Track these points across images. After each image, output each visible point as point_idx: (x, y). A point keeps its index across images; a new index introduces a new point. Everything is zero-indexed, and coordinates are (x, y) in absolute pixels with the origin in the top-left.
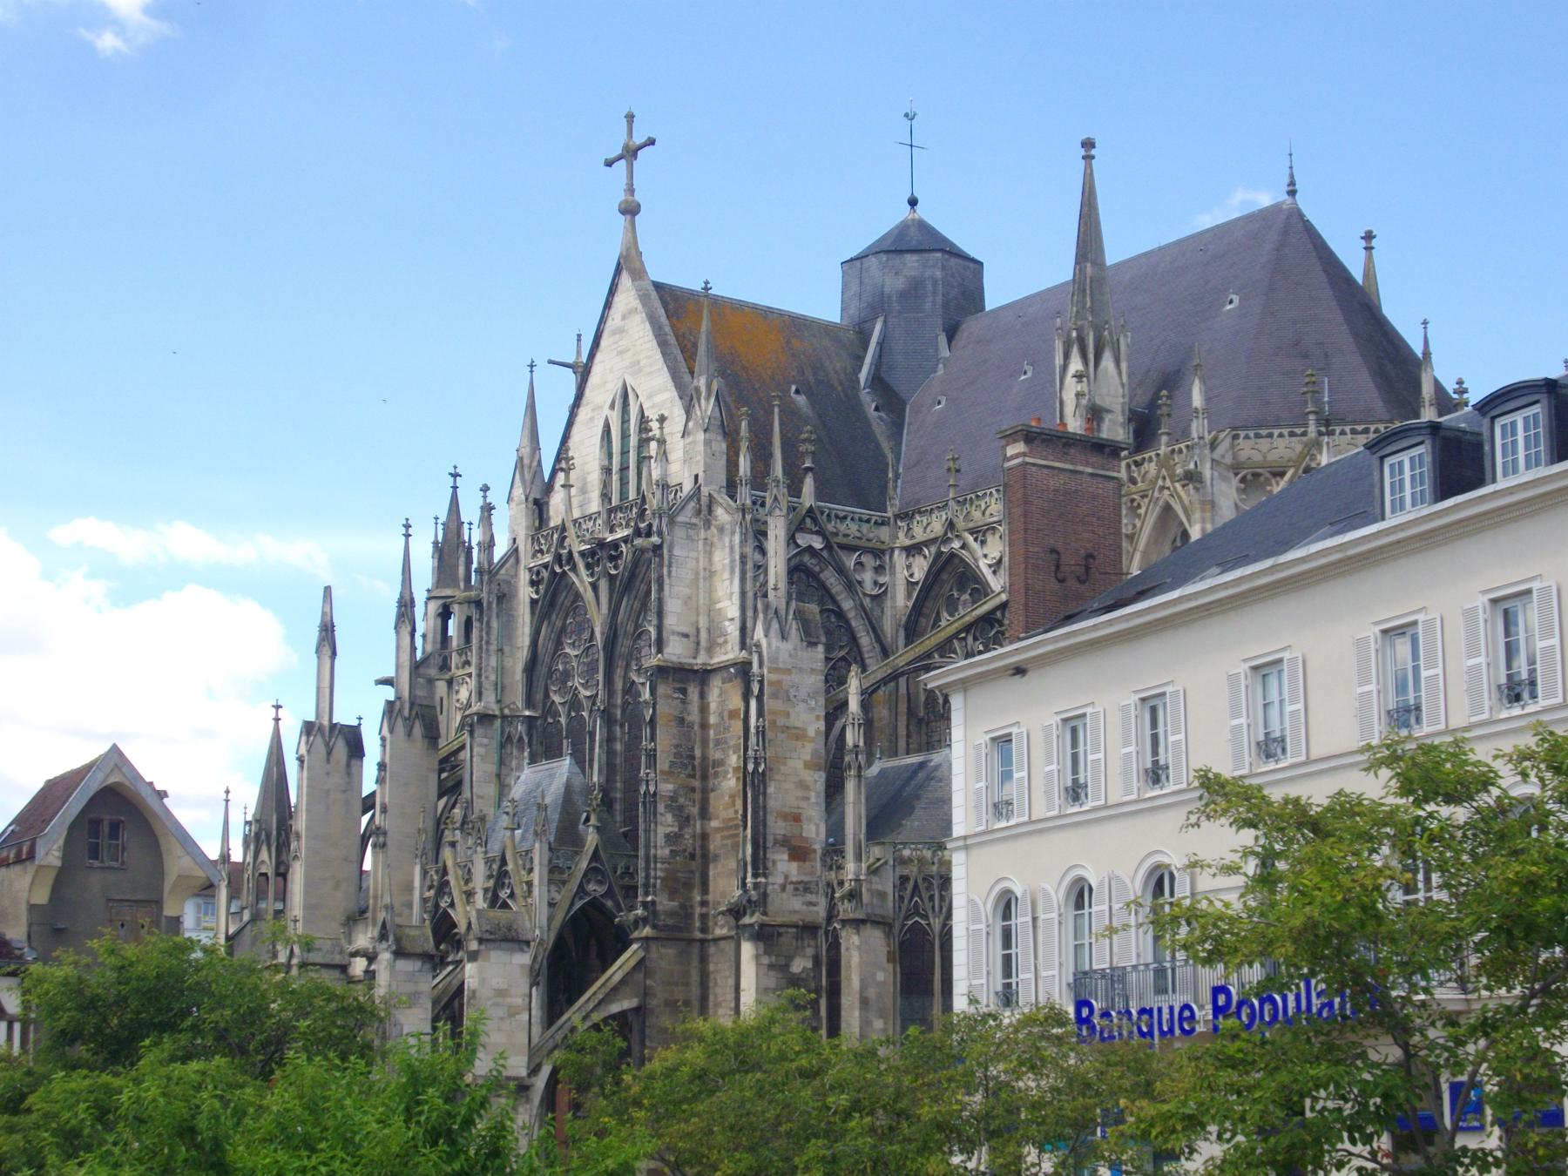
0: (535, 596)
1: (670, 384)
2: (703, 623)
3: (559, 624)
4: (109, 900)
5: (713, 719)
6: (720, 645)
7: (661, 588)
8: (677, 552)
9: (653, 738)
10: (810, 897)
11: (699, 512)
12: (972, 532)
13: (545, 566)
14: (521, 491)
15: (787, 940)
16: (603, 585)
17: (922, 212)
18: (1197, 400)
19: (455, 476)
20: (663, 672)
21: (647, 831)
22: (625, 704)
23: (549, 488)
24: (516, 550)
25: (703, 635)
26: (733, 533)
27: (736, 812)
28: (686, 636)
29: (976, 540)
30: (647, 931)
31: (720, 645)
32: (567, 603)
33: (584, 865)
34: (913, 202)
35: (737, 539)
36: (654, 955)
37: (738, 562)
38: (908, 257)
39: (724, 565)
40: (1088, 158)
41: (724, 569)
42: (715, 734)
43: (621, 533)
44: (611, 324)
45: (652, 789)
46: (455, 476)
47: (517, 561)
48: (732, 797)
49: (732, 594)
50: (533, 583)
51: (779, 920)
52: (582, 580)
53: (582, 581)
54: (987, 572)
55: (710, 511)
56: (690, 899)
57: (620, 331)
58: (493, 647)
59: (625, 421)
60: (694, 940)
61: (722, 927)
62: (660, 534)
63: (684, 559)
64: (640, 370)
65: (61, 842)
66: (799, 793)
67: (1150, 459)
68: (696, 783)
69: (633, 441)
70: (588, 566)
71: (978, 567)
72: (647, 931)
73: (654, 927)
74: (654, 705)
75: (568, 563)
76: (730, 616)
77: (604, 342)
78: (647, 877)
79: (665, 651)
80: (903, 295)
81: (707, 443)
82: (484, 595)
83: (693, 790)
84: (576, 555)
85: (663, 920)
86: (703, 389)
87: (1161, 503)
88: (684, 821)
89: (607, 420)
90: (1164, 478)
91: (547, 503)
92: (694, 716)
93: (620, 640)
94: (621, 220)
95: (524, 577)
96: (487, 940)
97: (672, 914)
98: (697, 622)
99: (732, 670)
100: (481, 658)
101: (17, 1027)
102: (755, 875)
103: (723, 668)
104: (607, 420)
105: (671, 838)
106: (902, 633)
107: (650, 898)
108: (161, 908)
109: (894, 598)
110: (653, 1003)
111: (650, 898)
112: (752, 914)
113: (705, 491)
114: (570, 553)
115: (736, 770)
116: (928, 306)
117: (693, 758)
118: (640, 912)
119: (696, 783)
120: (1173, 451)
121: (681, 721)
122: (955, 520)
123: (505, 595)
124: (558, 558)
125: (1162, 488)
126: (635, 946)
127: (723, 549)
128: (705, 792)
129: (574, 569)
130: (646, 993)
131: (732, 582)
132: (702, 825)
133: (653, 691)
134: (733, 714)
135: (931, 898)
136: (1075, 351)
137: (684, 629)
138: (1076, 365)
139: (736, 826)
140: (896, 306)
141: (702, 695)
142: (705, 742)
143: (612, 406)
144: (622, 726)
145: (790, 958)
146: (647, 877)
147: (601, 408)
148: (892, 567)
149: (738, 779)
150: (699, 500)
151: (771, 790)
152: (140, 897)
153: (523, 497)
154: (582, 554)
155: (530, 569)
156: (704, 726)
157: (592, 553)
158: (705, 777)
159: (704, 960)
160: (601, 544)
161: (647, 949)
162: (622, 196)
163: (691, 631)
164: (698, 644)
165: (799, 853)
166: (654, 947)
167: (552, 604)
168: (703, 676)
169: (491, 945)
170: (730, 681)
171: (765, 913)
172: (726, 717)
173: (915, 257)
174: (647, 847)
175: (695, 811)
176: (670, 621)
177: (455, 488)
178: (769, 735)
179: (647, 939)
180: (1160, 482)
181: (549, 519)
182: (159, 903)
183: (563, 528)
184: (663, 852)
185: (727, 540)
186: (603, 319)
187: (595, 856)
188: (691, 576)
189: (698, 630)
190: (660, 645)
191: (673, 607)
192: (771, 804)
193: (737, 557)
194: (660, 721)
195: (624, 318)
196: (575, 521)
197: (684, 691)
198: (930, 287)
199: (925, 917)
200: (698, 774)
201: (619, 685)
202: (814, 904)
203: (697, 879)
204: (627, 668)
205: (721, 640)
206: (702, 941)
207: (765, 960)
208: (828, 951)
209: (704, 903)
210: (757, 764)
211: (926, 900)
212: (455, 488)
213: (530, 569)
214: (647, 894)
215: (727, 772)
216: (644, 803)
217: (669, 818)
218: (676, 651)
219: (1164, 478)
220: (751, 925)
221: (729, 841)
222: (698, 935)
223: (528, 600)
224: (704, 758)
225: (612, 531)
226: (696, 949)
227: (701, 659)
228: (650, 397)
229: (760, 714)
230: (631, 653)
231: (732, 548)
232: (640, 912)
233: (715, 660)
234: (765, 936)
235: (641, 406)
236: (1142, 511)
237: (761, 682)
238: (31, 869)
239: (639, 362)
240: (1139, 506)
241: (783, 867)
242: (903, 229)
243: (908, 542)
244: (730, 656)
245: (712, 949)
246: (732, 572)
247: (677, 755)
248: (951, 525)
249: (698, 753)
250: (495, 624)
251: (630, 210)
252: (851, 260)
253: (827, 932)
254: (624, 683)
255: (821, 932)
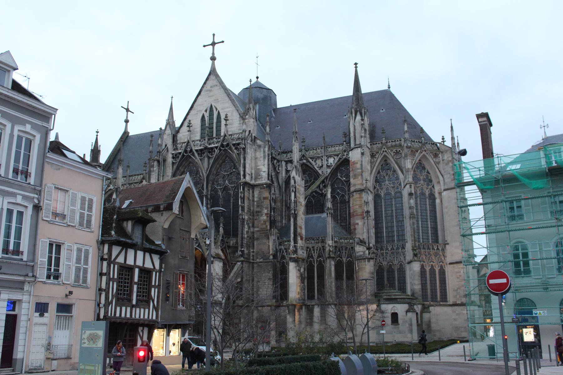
0: (174, 161)
1: (232, 106)
2: (253, 172)
3: (182, 170)
4: (180, 229)
5: (256, 199)
6: (259, 179)
7: (245, 160)
8: (248, 151)
9: (244, 203)
10: (303, 251)
11: (252, 141)
12: (311, 158)
13: (180, 153)
14: (170, 131)
15: (300, 262)
16: (206, 159)
17: (260, 80)
18: (406, 129)
19: (98, 132)
20: (246, 184)
21: (242, 230)
22: (211, 194)
23: (178, 131)
24: (167, 148)
25: (253, 175)
26: (265, 147)
27: (267, 226)
28: (249, 175)
29: (312, 160)
30: (242, 259)
31: (259, 179)
32: (186, 164)
33: (221, 238)
34: (257, 78)
35: (267, 149)
36: (244, 266)
37: (267, 156)
38: (264, 90)
39: (261, 157)
40: (356, 67)
41: (261, 157)
42: (257, 203)
43: (213, 146)
44: (205, 89)
45: (243, 217)
46: (98, 132)
47: (168, 151)
48: (265, 222)
49: (264, 165)
50: (173, 158)
51: (300, 257)
52: (197, 158)
53: (196, 158)
54: (317, 169)
55: (254, 141)
56: (250, 250)
57: (210, 91)
58: (162, 175)
59: (211, 114)
60: (250, 262)
61: (260, 259)
62: (245, 145)
63: (250, 152)
64: (218, 102)
65: (178, 206)
66: (301, 221)
67: (379, 143)
68: (251, 217)
69: (215, 120)
70: (198, 154)
71: (314, 167)
72: (242, 259)
73: (244, 258)
74: (244, 193)
75: (190, 153)
76: (263, 170)
77: (202, 93)
78: (242, 243)
79: (246, 178)
80: (263, 99)
81: (253, 122)
82: (160, 159)
83: (250, 219)
84: (194, 151)
85: (246, 256)
86: (252, 107)
87: (383, 155)
88: (249, 228)
89: (203, 114)
90: (384, 149)
91: (176, 136)
92: (251, 198)
93: (211, 176)
94: (211, 62)
95: (170, 156)
96: (216, 258)
97: (247, 254)
98: (251, 171)
99: (265, 186)
100: (158, 177)
101: (158, 274)
102: (295, 243)
103: (262, 185)
104: (203, 114)
105: (247, 232)
106: (284, 184)
107: (243, 249)
108: (190, 235)
109: (282, 174)
110: (244, 280)
111: (243, 249)
112: (294, 255)
113: (253, 135)
114: (191, 150)
115: (266, 214)
116: (269, 103)
117: (250, 209)
118: (240, 253)
119: (251, 217)
120: (387, 142)
121: (249, 199)
122: (305, 155)
123: (166, 160)
124: (186, 151)
125: (383, 151)
126: (239, 263)
127: (260, 151)
128: (254, 219)
129: (193, 155)
130: (242, 278)
131: (264, 161)
132: (253, 230)
133: (243, 189)
134: (265, 198)
135: (343, 253)
136: (358, 113)
137: (250, 173)
138: (359, 117)
139: (267, 230)
140: (261, 101)
141: (253, 192)
142: (253, 205)
143: (206, 111)
144: (210, 200)
145: (301, 268)
146: (242, 243)
147: (201, 111)
148: (282, 166)
149: (267, 217)
150: (252, 137)
151: (298, 219)
152: (186, 230)
153: (171, 133)
154: (197, 151)
155: (173, 154)
156: (253, 201)
157: (201, 150)
158: (253, 216)
159: (253, 268)
160: (206, 148)
161: (242, 264)
162: (211, 55)
163: (250, 173)
164: (252, 177)
165: (302, 239)
166: (244, 263)
167: (181, 164)
168: (253, 187)
169: (216, 259)
170: (264, 188)
171: (297, 255)
172: (262, 198)
173: (266, 90)
174: (242, 234)
175: (251, 225)
176: (247, 170)
177: (97, 135)
178: (297, 203)
179: (242, 261)
180: (383, 149)
181: (177, 140)
182: (189, 232)
183: (188, 142)
184: (246, 236)
185: (262, 150)
186: (203, 87)
187: (223, 237)
188: (250, 158)
189: (252, 174)
190: (244, 176)
191: (247, 166)
192: (298, 223)
193: (267, 154)
194: (246, 198)
195: (211, 87)
196: (194, 141)
197: (249, 190)
198: (269, 98)
199: (342, 258)
200: (252, 215)
201: (210, 188)
202: (303, 253)
203: (251, 245)
204: (213, 184)
205: (259, 177)
206: (253, 263)
207: (297, 268)
208: (307, 267)
209: (253, 252)
210: (295, 211)
211: (341, 252)
212: (97, 135)
213: (173, 154)
214: (242, 248)
215: (262, 215)
216: (241, 221)
217: (246, 226)
218: (248, 178)
219: (384, 149)
220: (294, 258)
221: (264, 235)
222: (252, 261)
223: (171, 162)
224: (254, 210)
225: (210, 144)
226: (251, 265)
227: (253, 182)
228: (222, 109)
229: (295, 197)
230: (214, 179)
231: (264, 152)
232: (240, 253)
233: (257, 183)
234: (296, 260)
235: (219, 112)
236: (377, 156)
237: (295, 188)
238: (166, 214)
239: (218, 99)
240: (375, 155)
241: (300, 242)
242: (257, 82)
243: (286, 160)
244: (264, 182)
245: (255, 265)
246: (264, 158)
247: (248, 208)
248: (303, 156)
249: (252, 208)
250: (162, 168)
251: (213, 59)
252: (246, 88)
253: (307, 261)
254: (211, 188)
255: (305, 261)
